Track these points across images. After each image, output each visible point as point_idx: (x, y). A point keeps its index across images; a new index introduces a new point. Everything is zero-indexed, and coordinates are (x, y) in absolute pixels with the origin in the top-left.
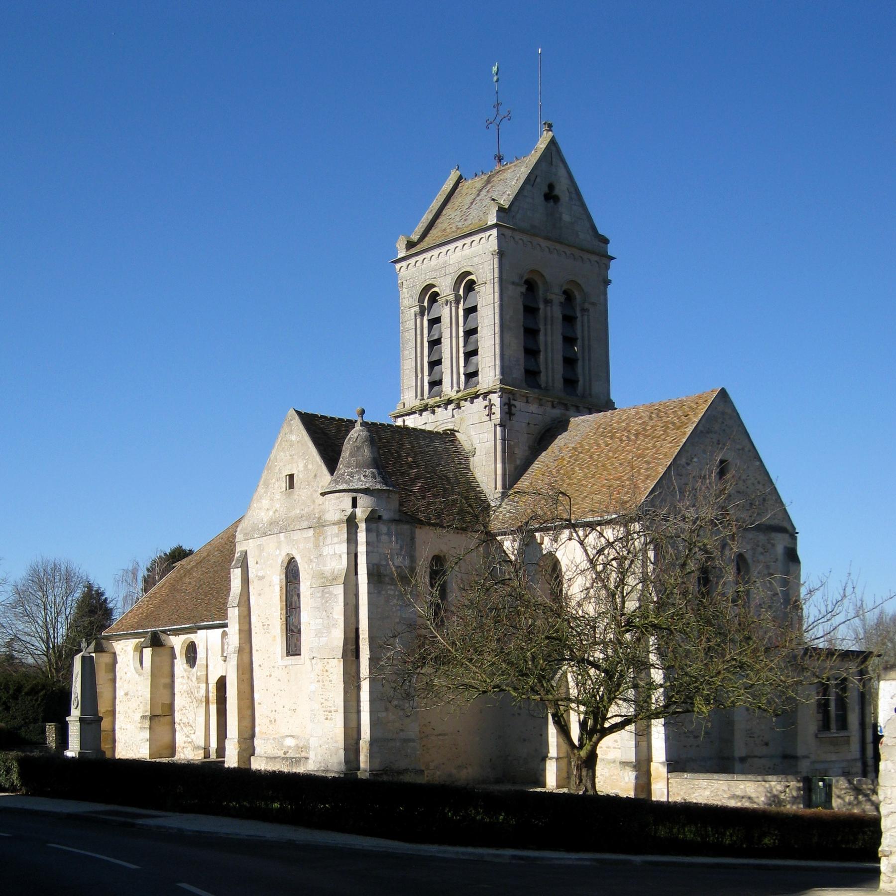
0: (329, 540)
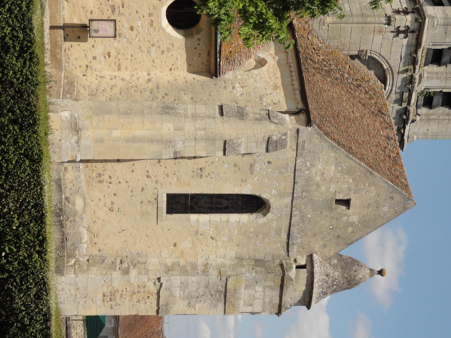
0: (268, 292)
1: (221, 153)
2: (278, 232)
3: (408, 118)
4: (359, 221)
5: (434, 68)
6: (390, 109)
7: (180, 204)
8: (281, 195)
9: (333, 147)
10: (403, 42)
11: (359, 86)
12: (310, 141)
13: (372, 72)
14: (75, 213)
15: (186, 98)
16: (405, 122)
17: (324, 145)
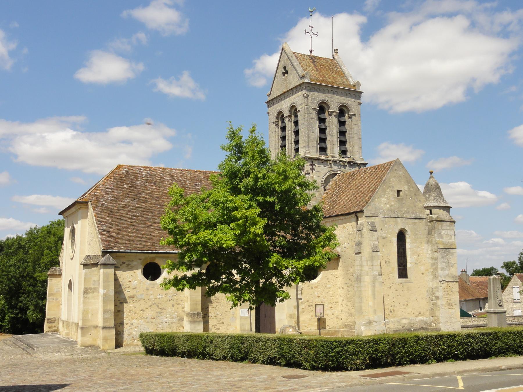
0: (444, 228)
1: (378, 253)
2: (414, 224)
3: (353, 162)
4: (407, 185)
5: (328, 151)
6: (349, 171)
7: (403, 272)
8: (396, 223)
9: (373, 199)
10: (317, 166)
11: (339, 186)
12: (370, 210)
13: (331, 180)
14: (410, 323)
15: (351, 270)
16: (355, 163)
17: (372, 203)
